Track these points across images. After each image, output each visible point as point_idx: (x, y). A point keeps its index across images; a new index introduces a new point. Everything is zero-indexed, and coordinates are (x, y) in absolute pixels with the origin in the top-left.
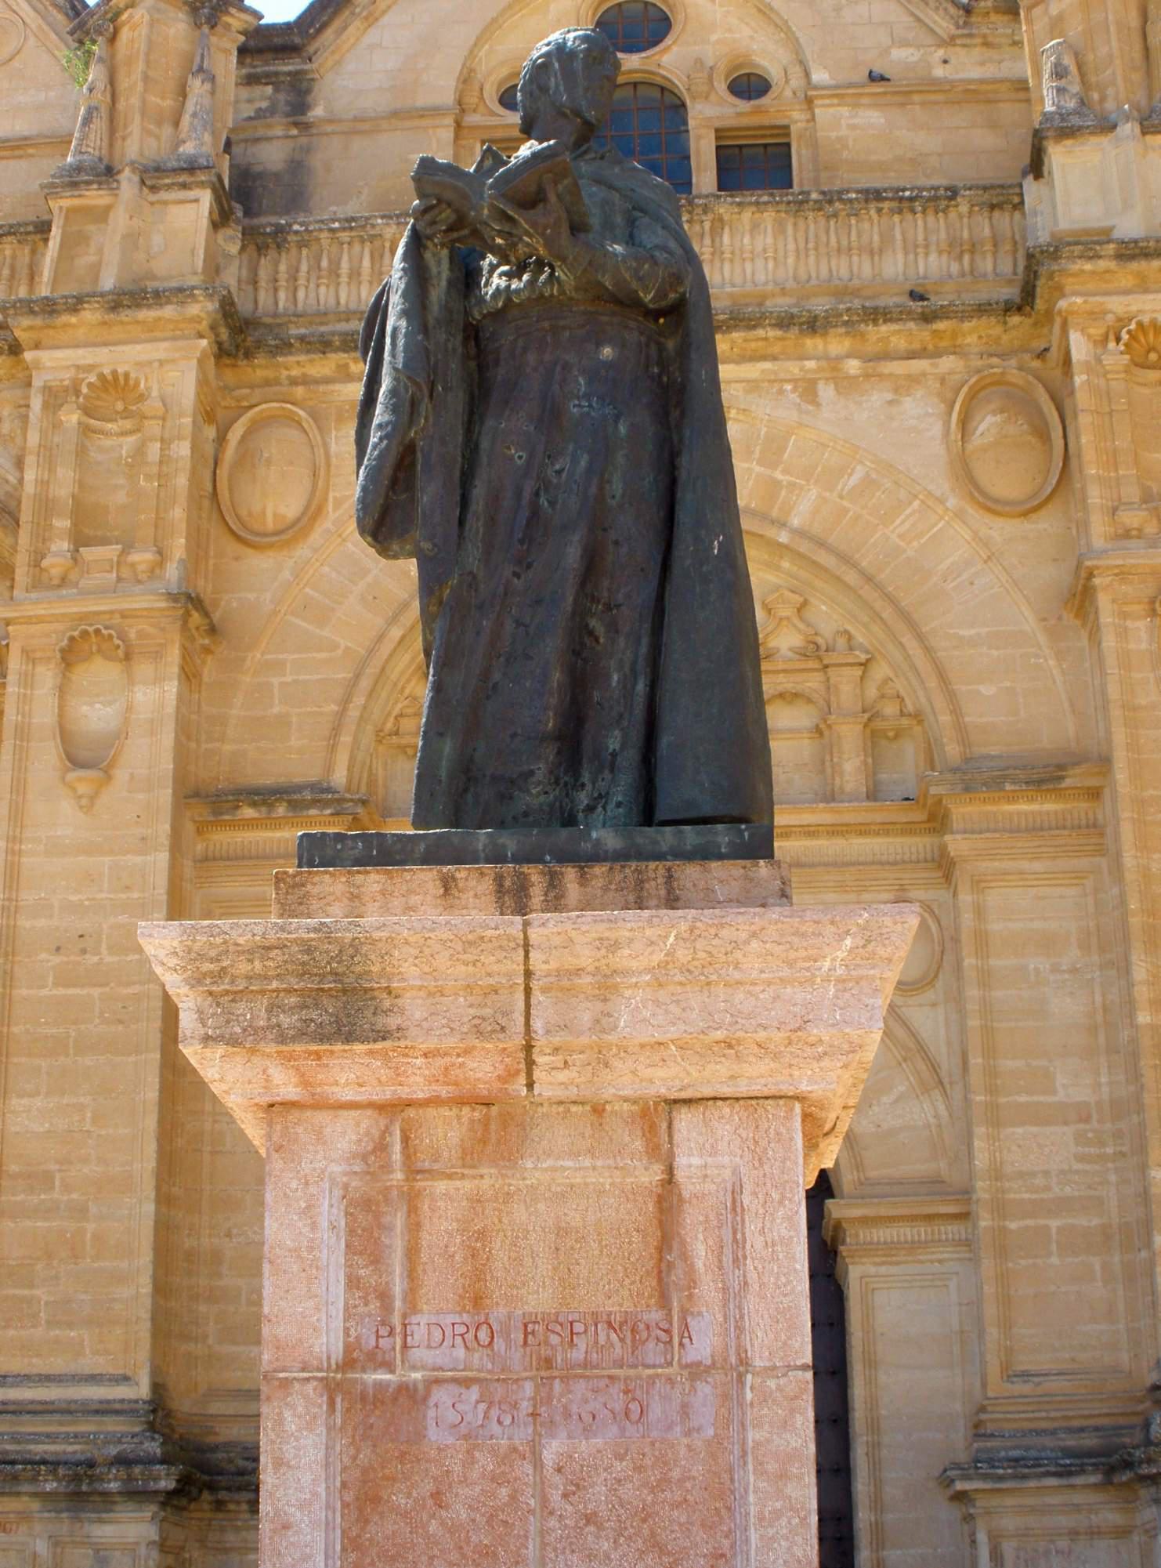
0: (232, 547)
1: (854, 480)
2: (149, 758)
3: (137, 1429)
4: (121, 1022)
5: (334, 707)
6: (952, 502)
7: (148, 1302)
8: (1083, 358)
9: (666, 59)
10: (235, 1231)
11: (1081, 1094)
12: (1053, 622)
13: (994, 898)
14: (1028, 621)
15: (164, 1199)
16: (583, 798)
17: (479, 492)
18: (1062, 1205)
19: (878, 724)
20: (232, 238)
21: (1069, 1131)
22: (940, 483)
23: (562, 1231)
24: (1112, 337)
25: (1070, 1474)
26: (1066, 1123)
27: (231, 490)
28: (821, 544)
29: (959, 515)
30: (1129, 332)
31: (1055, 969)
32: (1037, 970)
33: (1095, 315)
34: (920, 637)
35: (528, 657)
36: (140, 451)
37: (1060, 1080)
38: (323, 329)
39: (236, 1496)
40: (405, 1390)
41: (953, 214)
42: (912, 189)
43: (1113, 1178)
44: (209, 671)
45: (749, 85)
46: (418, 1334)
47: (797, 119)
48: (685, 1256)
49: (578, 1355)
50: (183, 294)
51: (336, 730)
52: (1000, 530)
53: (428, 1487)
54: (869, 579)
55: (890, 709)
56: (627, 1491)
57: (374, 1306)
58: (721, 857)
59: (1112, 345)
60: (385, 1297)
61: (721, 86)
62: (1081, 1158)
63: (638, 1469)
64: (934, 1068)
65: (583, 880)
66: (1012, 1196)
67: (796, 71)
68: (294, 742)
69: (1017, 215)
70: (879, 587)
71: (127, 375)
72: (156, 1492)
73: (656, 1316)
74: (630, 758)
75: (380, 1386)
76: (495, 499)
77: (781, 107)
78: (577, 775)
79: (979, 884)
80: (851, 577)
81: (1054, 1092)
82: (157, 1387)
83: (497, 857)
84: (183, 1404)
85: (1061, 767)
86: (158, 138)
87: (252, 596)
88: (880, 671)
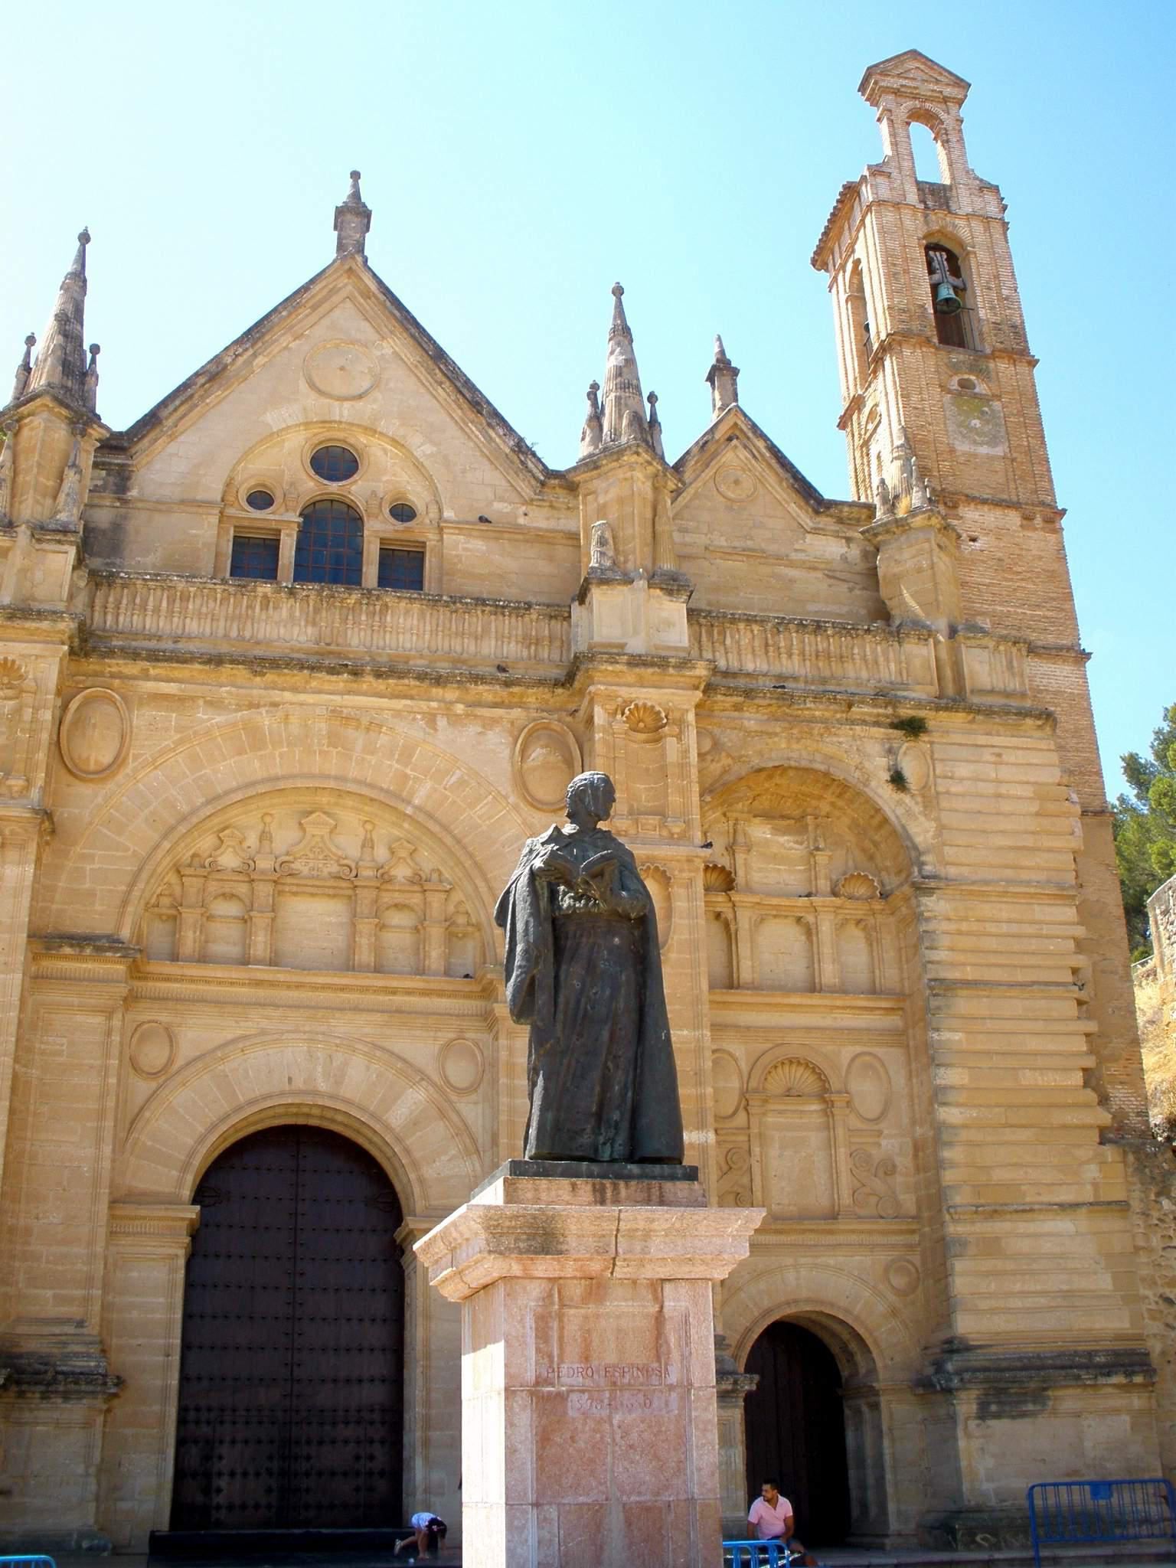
0: (67, 778)
1: (454, 779)
5: (124, 888)
8: (601, 722)
9: (353, 488)
16: (601, 1139)
17: (561, 999)
19: (454, 929)
20: (82, 577)
22: (506, 787)
23: (619, 1331)
27: (68, 741)
28: (431, 816)
29: (516, 808)
33: (610, 697)
34: (487, 881)
36: (18, 710)
38: (134, 644)
39: (33, 1388)
40: (559, 1394)
41: (527, 618)
45: (403, 512)
46: (564, 1371)
47: (431, 538)
48: (667, 1342)
49: (626, 1381)
51: (125, 903)
53: (568, 1435)
54: (459, 842)
55: (461, 920)
56: (646, 1435)
57: (546, 1360)
58: (679, 1179)
59: (619, 716)
60: (550, 1357)
61: (386, 511)
63: (650, 1427)
64: (474, 1141)
65: (627, 1186)
67: (433, 509)
68: (98, 907)
71: (13, 662)
73: (656, 1365)
74: (625, 1125)
75: (549, 1392)
76: (567, 1003)
77: (421, 530)
78: (599, 1128)
80: (448, 840)
83: (590, 1175)
86: (42, 505)
87: (77, 811)
88: (458, 896)
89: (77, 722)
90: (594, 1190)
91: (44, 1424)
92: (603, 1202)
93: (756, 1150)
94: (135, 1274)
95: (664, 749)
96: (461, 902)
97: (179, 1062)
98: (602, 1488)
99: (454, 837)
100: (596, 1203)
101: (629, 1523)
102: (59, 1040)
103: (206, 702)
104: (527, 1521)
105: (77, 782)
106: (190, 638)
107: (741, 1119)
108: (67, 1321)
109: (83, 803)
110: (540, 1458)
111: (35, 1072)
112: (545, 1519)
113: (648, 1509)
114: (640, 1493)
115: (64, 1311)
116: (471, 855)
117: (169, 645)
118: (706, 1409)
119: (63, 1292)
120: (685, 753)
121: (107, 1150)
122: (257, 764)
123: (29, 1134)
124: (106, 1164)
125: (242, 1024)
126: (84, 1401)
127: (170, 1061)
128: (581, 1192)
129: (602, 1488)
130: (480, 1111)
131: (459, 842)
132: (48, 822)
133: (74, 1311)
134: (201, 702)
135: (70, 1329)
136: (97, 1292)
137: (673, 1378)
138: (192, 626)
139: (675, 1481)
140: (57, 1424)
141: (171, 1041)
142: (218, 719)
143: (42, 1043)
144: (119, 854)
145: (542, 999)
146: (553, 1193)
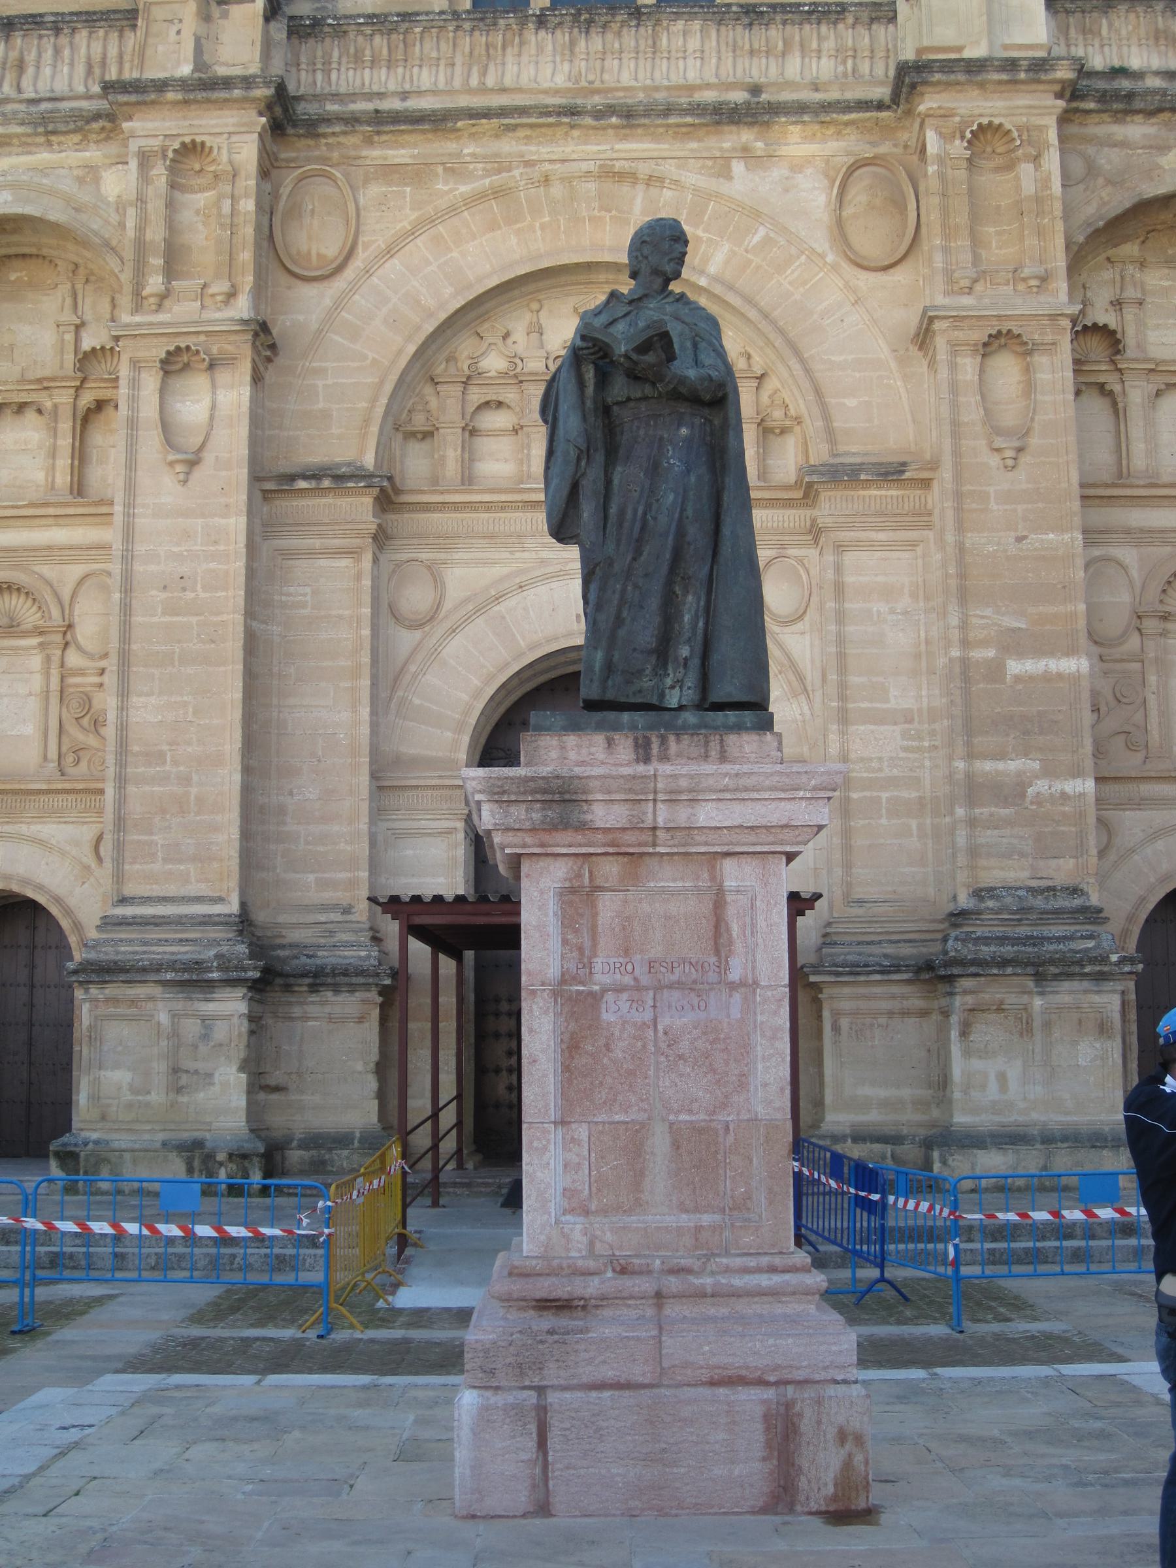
0: (284, 279)
1: (757, 238)
2: (231, 446)
3: (231, 935)
4: (213, 642)
5: (365, 405)
6: (830, 258)
7: (237, 844)
8: (935, 151)
10: (295, 791)
11: (908, 703)
12: (902, 352)
13: (849, 558)
14: (884, 352)
15: (247, 770)
16: (669, 682)
17: (613, 510)
18: (892, 782)
19: (769, 424)
21: (898, 728)
22: (821, 242)
23: (668, 918)
24: (958, 135)
25: (889, 972)
26: (895, 724)
27: (283, 235)
28: (731, 288)
29: (835, 268)
30: (972, 132)
31: (892, 611)
32: (879, 611)
33: (947, 115)
34: (802, 361)
35: (642, 607)
36: (218, 203)
37: (893, 692)
39: (300, 981)
40: (591, 994)
41: (841, 26)
42: (810, 5)
43: (927, 763)
44: (270, 376)
46: (598, 967)
48: (728, 930)
49: (674, 978)
50: (247, 82)
51: (367, 422)
52: (865, 280)
53: (602, 1042)
54: (766, 316)
55: (778, 414)
56: (699, 1044)
57: (575, 954)
58: (747, 729)
59: (957, 142)
60: (581, 949)
62: (906, 749)
63: (704, 1033)
64: (801, 679)
65: (678, 741)
66: (854, 774)
68: (335, 431)
69: (891, 27)
70: (773, 322)
72: (246, 980)
73: (713, 959)
74: (696, 662)
75: (579, 993)
76: (622, 513)
78: (666, 669)
79: (840, 548)
80: (752, 314)
81: (887, 701)
82: (243, 905)
83: (634, 728)
84: (260, 916)
85: (904, 464)
87: (301, 318)
88: (772, 384)
89: (294, 211)
90: (637, 746)
91: (315, 1019)
92: (647, 760)
93: (1152, 679)
94: (410, 852)
95: (1017, 178)
96: (776, 391)
97: (448, 605)
98: (644, 1105)
99: (760, 311)
100: (637, 761)
101: (676, 1146)
102: (301, 590)
103: (445, 169)
104: (549, 1141)
105: (299, 283)
106: (420, 93)
107: (1134, 642)
108: (333, 907)
109: (307, 306)
110: (566, 1068)
111: (276, 629)
112: (573, 1140)
113: (701, 1131)
114: (690, 1112)
115: (328, 896)
116: (781, 332)
117: (395, 104)
118: (775, 1013)
119: (326, 875)
120: (1046, 182)
121: (365, 712)
122: (514, 240)
123: (275, 701)
124: (365, 730)
125: (518, 555)
126: (357, 994)
127: (439, 606)
128: (620, 749)
129: (644, 1105)
130: (808, 643)
131: (766, 316)
132: (264, 337)
133: (340, 896)
134: (440, 169)
135: (336, 916)
136: (364, 875)
137: (735, 975)
138: (425, 78)
139: (735, 1098)
140: (330, 1019)
141: (435, 581)
142: (463, 189)
143: (282, 594)
144: (356, 364)
145: (587, 511)
146: (584, 751)
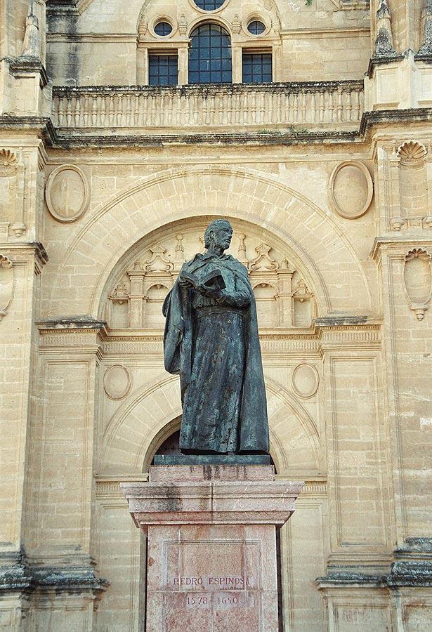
1: (291, 203)
2: (23, 309)
3: (14, 564)
4: (11, 407)
6: (328, 213)
7: (20, 514)
9: (223, 14)
10: (52, 485)
11: (370, 439)
12: (365, 260)
13: (338, 365)
14: (356, 261)
15: (27, 474)
18: (362, 480)
19: (297, 297)
21: (364, 453)
22: (324, 205)
24: (394, 150)
25: (363, 583)
26: (363, 450)
27: (51, 199)
28: (278, 228)
30: (401, 148)
31: (361, 392)
32: (353, 392)
35: (209, 405)
36: (16, 183)
37: (362, 434)
38: (87, 134)
39: (50, 588)
41: (335, 93)
42: (319, 83)
43: (380, 471)
44: (43, 271)
45: (256, 25)
47: (275, 46)
49: (221, 586)
50: (32, 120)
51: (94, 295)
52: (346, 224)
55: (302, 292)
58: (257, 464)
59: (394, 153)
61: (245, 28)
62: (369, 463)
64: (315, 426)
66: (342, 476)
67: (276, 22)
69: (361, 93)
70: (299, 246)
72: (21, 588)
77: (269, 37)
79: (333, 359)
80: (289, 242)
81: (359, 438)
82: (22, 547)
84: (30, 552)
85: (366, 317)
87: (60, 242)
88: (299, 276)
89: (58, 186)
92: (209, 478)
108: (71, 547)
115: (68, 540)
116: (303, 250)
117: (109, 134)
121: (90, 443)
123: (43, 438)
124: (90, 452)
131: (295, 243)
133: (75, 540)
138: (123, 121)
